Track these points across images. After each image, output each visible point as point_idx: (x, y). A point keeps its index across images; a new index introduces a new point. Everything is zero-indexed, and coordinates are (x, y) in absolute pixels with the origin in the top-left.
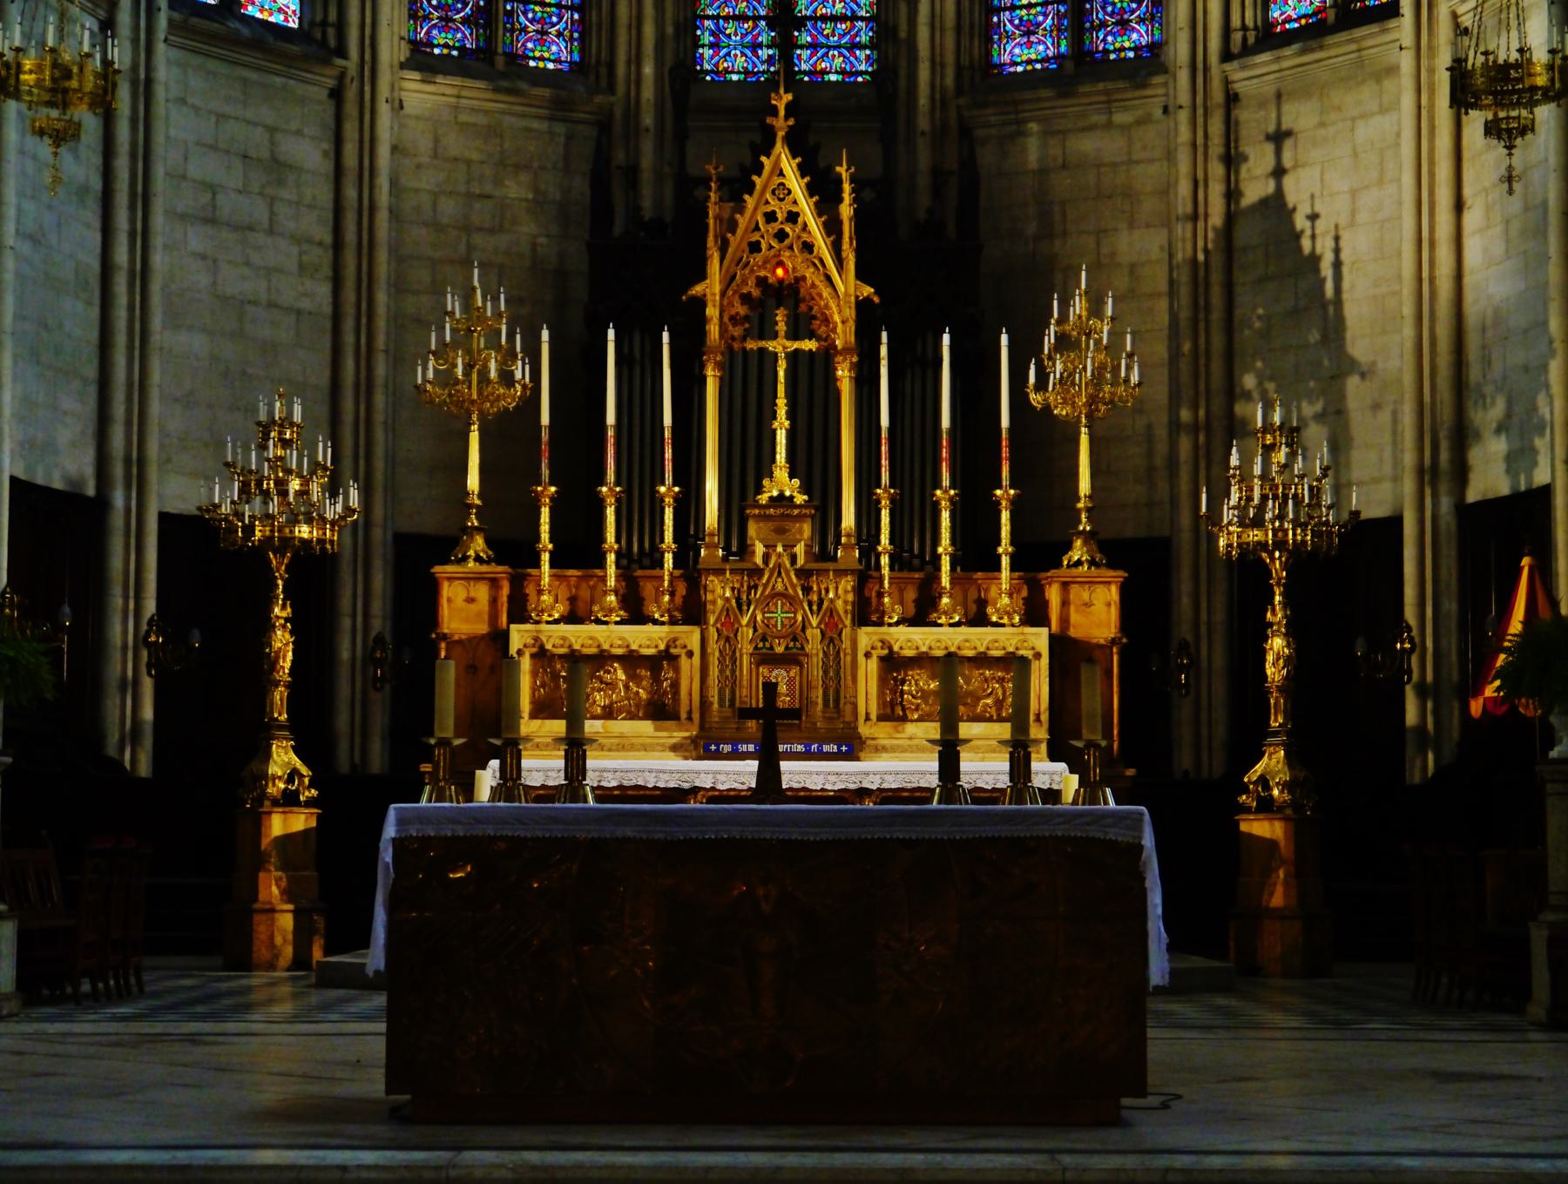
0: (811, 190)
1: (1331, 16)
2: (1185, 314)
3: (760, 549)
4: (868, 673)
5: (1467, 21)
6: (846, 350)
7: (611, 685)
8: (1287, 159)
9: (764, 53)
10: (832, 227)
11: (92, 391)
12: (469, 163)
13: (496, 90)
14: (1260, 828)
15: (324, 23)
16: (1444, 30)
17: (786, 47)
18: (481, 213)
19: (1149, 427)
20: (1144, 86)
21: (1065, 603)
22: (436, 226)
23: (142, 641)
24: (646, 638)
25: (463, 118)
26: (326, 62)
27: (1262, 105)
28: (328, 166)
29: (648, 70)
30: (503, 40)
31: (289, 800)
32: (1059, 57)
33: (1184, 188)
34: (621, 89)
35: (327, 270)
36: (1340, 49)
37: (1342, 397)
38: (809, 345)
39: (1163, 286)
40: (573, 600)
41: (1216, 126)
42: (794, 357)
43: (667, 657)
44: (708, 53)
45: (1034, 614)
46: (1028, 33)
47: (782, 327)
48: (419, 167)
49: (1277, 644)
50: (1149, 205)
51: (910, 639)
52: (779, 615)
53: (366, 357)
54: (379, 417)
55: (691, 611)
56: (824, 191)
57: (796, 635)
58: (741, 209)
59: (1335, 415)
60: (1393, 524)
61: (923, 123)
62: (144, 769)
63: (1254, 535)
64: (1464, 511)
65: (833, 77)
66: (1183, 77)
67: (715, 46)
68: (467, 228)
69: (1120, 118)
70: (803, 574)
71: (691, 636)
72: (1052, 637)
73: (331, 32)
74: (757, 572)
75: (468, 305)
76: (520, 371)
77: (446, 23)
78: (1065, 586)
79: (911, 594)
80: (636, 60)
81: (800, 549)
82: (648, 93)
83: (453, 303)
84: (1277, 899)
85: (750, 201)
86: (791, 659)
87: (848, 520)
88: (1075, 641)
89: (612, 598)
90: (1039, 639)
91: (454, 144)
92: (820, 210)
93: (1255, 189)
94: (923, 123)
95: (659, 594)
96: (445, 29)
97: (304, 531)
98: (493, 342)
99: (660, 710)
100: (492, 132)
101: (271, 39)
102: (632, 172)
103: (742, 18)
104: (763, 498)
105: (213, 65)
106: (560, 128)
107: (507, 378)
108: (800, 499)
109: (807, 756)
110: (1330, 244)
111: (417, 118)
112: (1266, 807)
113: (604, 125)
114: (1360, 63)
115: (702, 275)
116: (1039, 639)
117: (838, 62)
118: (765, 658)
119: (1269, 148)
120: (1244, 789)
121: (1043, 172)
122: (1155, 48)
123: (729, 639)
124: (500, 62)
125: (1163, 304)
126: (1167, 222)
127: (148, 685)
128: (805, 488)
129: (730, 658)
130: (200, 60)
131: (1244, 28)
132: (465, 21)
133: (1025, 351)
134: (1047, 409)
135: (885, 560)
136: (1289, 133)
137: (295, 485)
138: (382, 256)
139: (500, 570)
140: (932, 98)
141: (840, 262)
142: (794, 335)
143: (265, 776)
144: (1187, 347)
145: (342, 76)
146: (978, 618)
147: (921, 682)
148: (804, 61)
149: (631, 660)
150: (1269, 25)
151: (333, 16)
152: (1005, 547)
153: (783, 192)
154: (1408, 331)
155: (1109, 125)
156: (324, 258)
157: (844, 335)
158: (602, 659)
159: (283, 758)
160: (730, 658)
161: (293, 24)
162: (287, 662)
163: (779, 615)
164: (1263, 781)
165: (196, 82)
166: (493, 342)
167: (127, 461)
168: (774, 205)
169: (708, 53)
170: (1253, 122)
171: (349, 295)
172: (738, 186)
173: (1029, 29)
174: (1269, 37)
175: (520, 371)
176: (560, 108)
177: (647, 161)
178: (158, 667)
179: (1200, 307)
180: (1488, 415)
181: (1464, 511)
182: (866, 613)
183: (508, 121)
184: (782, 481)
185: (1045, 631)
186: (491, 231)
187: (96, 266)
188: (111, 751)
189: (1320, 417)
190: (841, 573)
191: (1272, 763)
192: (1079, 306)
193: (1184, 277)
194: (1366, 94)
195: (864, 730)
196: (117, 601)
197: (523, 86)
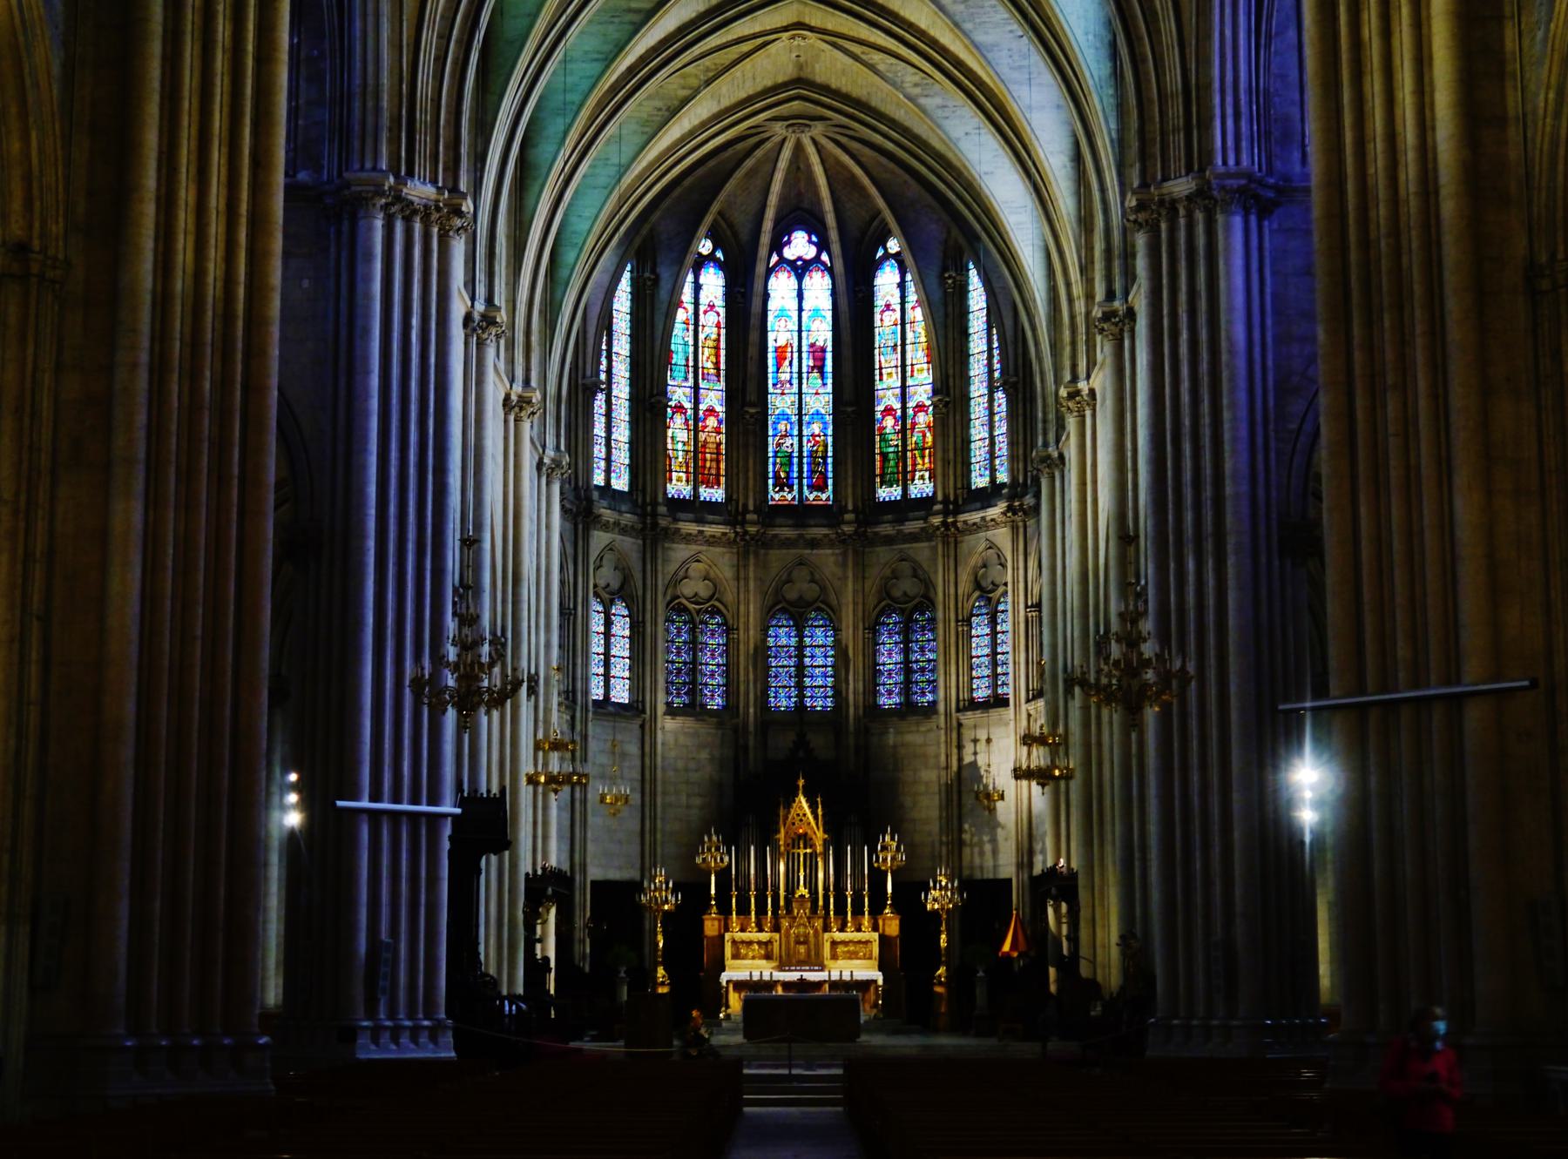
0: (810, 807)
1: (992, 700)
2: (944, 802)
3: (796, 911)
4: (827, 946)
5: (1031, 712)
6: (820, 854)
7: (754, 950)
8: (978, 749)
9: (793, 700)
10: (816, 818)
11: (569, 842)
12: (687, 746)
13: (697, 720)
14: (939, 989)
15: (638, 701)
16: (1024, 716)
17: (801, 696)
18: (692, 765)
19: (933, 842)
20: (930, 718)
21: (884, 925)
22: (676, 770)
23: (586, 926)
24: (764, 936)
25: (686, 730)
26: (638, 716)
27: (970, 729)
28: (640, 752)
29: (751, 710)
30: (699, 698)
31: (663, 984)
32: (900, 704)
33: (943, 758)
34: (741, 717)
35: (639, 789)
36: (995, 713)
37: (996, 835)
38: (808, 851)
39: (936, 789)
40: (742, 925)
41: (954, 735)
42: (805, 854)
43: (770, 942)
44: (773, 700)
45: (875, 928)
46: (890, 694)
47: (802, 846)
48: (670, 749)
49: (943, 936)
50: (932, 761)
51: (839, 936)
52: (802, 930)
53: (654, 819)
54: (659, 842)
55: (776, 928)
56: (813, 807)
57: (806, 936)
58: (789, 812)
59: (994, 841)
60: (1010, 880)
61: (851, 728)
62: (587, 969)
63: (936, 906)
64: (1031, 877)
65: (819, 709)
66: (942, 718)
67: (775, 697)
68: (687, 770)
69: (922, 729)
70: (809, 918)
71: (777, 936)
72: (880, 936)
73: (640, 705)
74: (795, 918)
75: (710, 839)
76: (726, 859)
77: (678, 695)
78: (884, 920)
79: (840, 922)
80: (747, 706)
81: (807, 911)
82: (751, 718)
83: (706, 839)
84: (943, 1010)
85: (792, 811)
86: (805, 942)
87: (821, 903)
88: (886, 936)
89: (753, 925)
90: (876, 936)
91: (682, 739)
92: (812, 813)
93: (968, 759)
94: (851, 728)
95: (766, 924)
96: (678, 697)
97: (666, 907)
98: (718, 849)
99: (768, 957)
100: (696, 734)
101: (622, 712)
102: (746, 748)
103: (785, 687)
104: (797, 896)
105: (605, 723)
106: (720, 732)
107: (722, 860)
108: (807, 896)
109: (810, 970)
110: (992, 781)
111: (670, 732)
112: (940, 983)
113: (735, 730)
114: (1001, 719)
115: (778, 832)
116: (876, 936)
117: (821, 703)
118: (798, 943)
119: (972, 745)
120: (935, 978)
121: (895, 747)
122: (934, 703)
123: (788, 935)
124: (698, 708)
125: (937, 797)
126: (938, 767)
127: (588, 941)
128: (810, 892)
129: (788, 942)
130: (599, 722)
131: (964, 700)
132: (685, 693)
133: (872, 851)
134: (879, 868)
135: (832, 913)
136: (978, 740)
137: (664, 893)
138: (659, 783)
139: (722, 917)
140: (855, 719)
141: (818, 828)
142: (805, 848)
143: (655, 977)
144: (944, 814)
145: (644, 720)
146: (859, 930)
147: (840, 949)
148: (808, 703)
149: (760, 943)
150: (973, 699)
151: (640, 699)
152: (866, 908)
153: (801, 808)
154: (1013, 817)
155: (918, 731)
156: (637, 785)
157: (819, 849)
158: (750, 943)
159: (661, 971)
160: (788, 942)
161: (627, 701)
162: (661, 945)
163: (802, 930)
164: (940, 976)
165: (598, 730)
166: (718, 849)
167: (580, 865)
168: (799, 812)
169: (773, 700)
170: (968, 734)
171: (647, 799)
172: (788, 806)
173: (890, 692)
174: (973, 705)
175: (726, 859)
176: (720, 725)
177: (751, 743)
178: (593, 935)
179: (949, 800)
180: (1038, 847)
181: (1031, 877)
182: (827, 928)
183: (703, 730)
184: (802, 891)
185: (877, 934)
186: (696, 771)
187: (569, 798)
188: (577, 962)
189: (990, 841)
190: (819, 918)
191: (942, 970)
192: (887, 838)
193: (943, 788)
194: (1003, 729)
195: (826, 962)
196: (577, 912)
197: (706, 718)
